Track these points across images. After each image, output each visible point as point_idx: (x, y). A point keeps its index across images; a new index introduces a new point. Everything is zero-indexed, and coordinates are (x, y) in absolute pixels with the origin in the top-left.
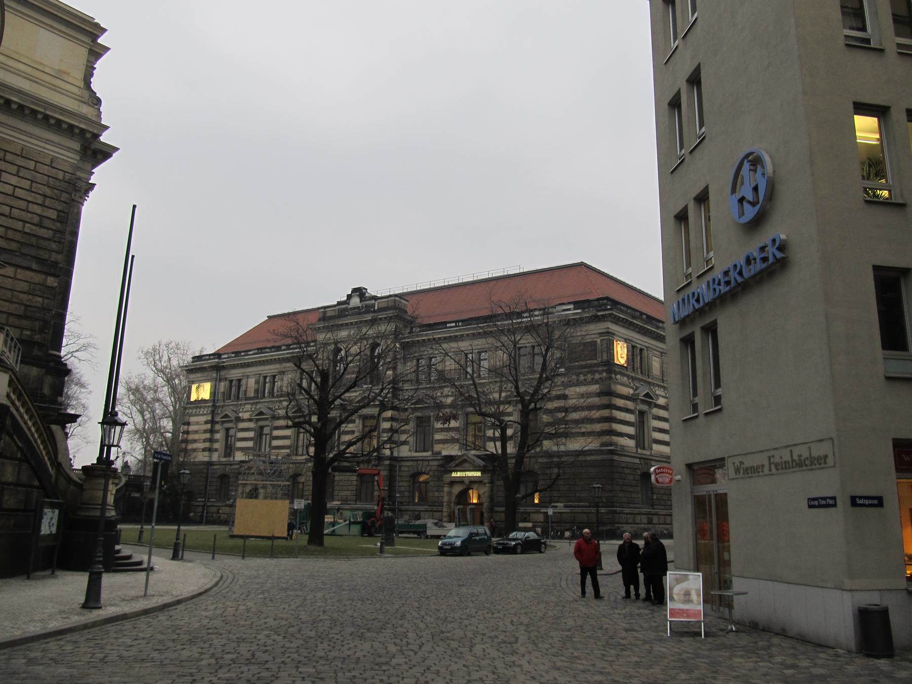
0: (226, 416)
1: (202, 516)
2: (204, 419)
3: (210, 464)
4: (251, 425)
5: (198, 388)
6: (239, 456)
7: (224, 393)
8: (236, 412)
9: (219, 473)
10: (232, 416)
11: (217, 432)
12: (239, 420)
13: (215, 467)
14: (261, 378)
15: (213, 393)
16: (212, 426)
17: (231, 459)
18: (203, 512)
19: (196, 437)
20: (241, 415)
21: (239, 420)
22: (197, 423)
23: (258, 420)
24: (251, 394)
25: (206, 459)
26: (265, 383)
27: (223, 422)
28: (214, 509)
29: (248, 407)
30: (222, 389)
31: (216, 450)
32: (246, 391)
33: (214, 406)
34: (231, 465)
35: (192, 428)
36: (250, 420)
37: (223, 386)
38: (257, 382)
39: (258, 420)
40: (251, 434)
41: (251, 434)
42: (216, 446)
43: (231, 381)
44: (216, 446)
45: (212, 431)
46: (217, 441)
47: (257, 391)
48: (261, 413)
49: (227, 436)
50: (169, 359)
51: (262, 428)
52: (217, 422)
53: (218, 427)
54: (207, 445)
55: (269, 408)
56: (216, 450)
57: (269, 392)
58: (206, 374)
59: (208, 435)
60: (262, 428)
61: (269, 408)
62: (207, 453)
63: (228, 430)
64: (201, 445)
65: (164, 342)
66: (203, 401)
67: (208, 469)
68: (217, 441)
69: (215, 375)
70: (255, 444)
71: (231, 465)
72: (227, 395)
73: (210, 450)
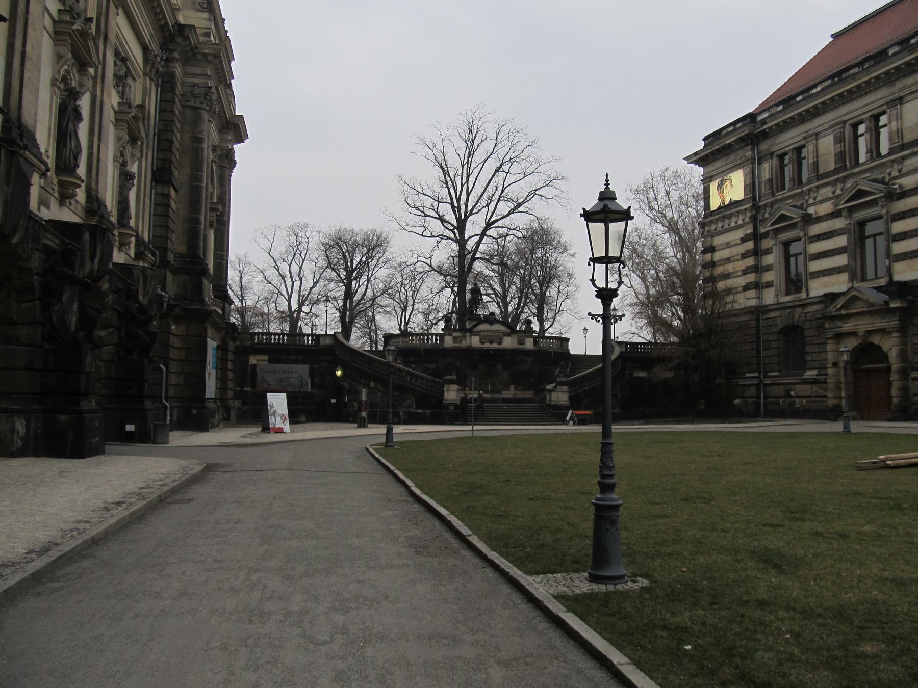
0: (783, 218)
1: (757, 404)
2: (740, 234)
3: (760, 311)
4: (839, 223)
5: (720, 186)
6: (818, 288)
7: (770, 181)
8: (801, 207)
9: (780, 324)
10: (796, 215)
11: (768, 251)
12: (809, 220)
13: (772, 315)
14: (848, 129)
15: (751, 187)
16: (756, 245)
17: (803, 295)
18: (758, 397)
19: (730, 267)
20: (811, 210)
21: (809, 220)
22: (728, 245)
23: (851, 210)
24: (829, 164)
25: (753, 303)
26: (856, 137)
27: (777, 232)
28: (780, 390)
29: (826, 191)
30: (766, 175)
31: (769, 285)
32: (816, 165)
33: (755, 207)
34: (804, 306)
35: (718, 256)
36: (835, 214)
37: (766, 170)
38: (839, 139)
39: (851, 210)
40: (842, 241)
41: (842, 241)
42: (768, 277)
43: (781, 157)
44: (768, 277)
45: (757, 253)
46: (768, 268)
47: (840, 157)
48: (861, 193)
49: (787, 257)
50: (667, 193)
51: (862, 224)
52: (766, 235)
53: (766, 243)
54: (751, 278)
55: (873, 181)
56: (769, 285)
57: (869, 151)
58: (732, 157)
59: (750, 261)
60: (862, 224)
61: (873, 181)
62: (752, 293)
63: (787, 244)
64: (741, 281)
65: (657, 173)
66: (734, 204)
67: (758, 320)
68: (768, 268)
69: (749, 154)
70: (852, 257)
71: (804, 306)
72: (778, 183)
73: (757, 286)
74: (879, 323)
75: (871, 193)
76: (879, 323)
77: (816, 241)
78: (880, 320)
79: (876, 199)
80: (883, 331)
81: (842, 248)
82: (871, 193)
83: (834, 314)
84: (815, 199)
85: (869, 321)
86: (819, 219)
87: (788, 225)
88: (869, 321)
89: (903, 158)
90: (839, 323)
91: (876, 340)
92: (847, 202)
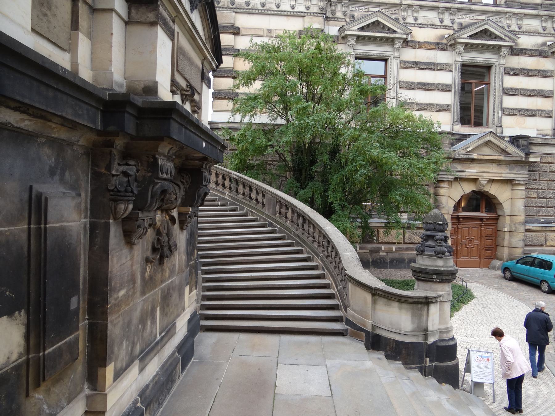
36: (439, 46)
41: (446, 78)
74: (506, 173)
75: (501, 39)
76: (506, 173)
77: (412, 68)
78: (507, 171)
79: (500, 47)
80: (510, 182)
81: (447, 85)
82: (497, 38)
83: (462, 156)
84: (416, 19)
85: (495, 170)
86: (421, 45)
87: (381, 38)
88: (495, 170)
89: (526, 16)
90: (459, 167)
91: (493, 190)
92: (471, 37)
